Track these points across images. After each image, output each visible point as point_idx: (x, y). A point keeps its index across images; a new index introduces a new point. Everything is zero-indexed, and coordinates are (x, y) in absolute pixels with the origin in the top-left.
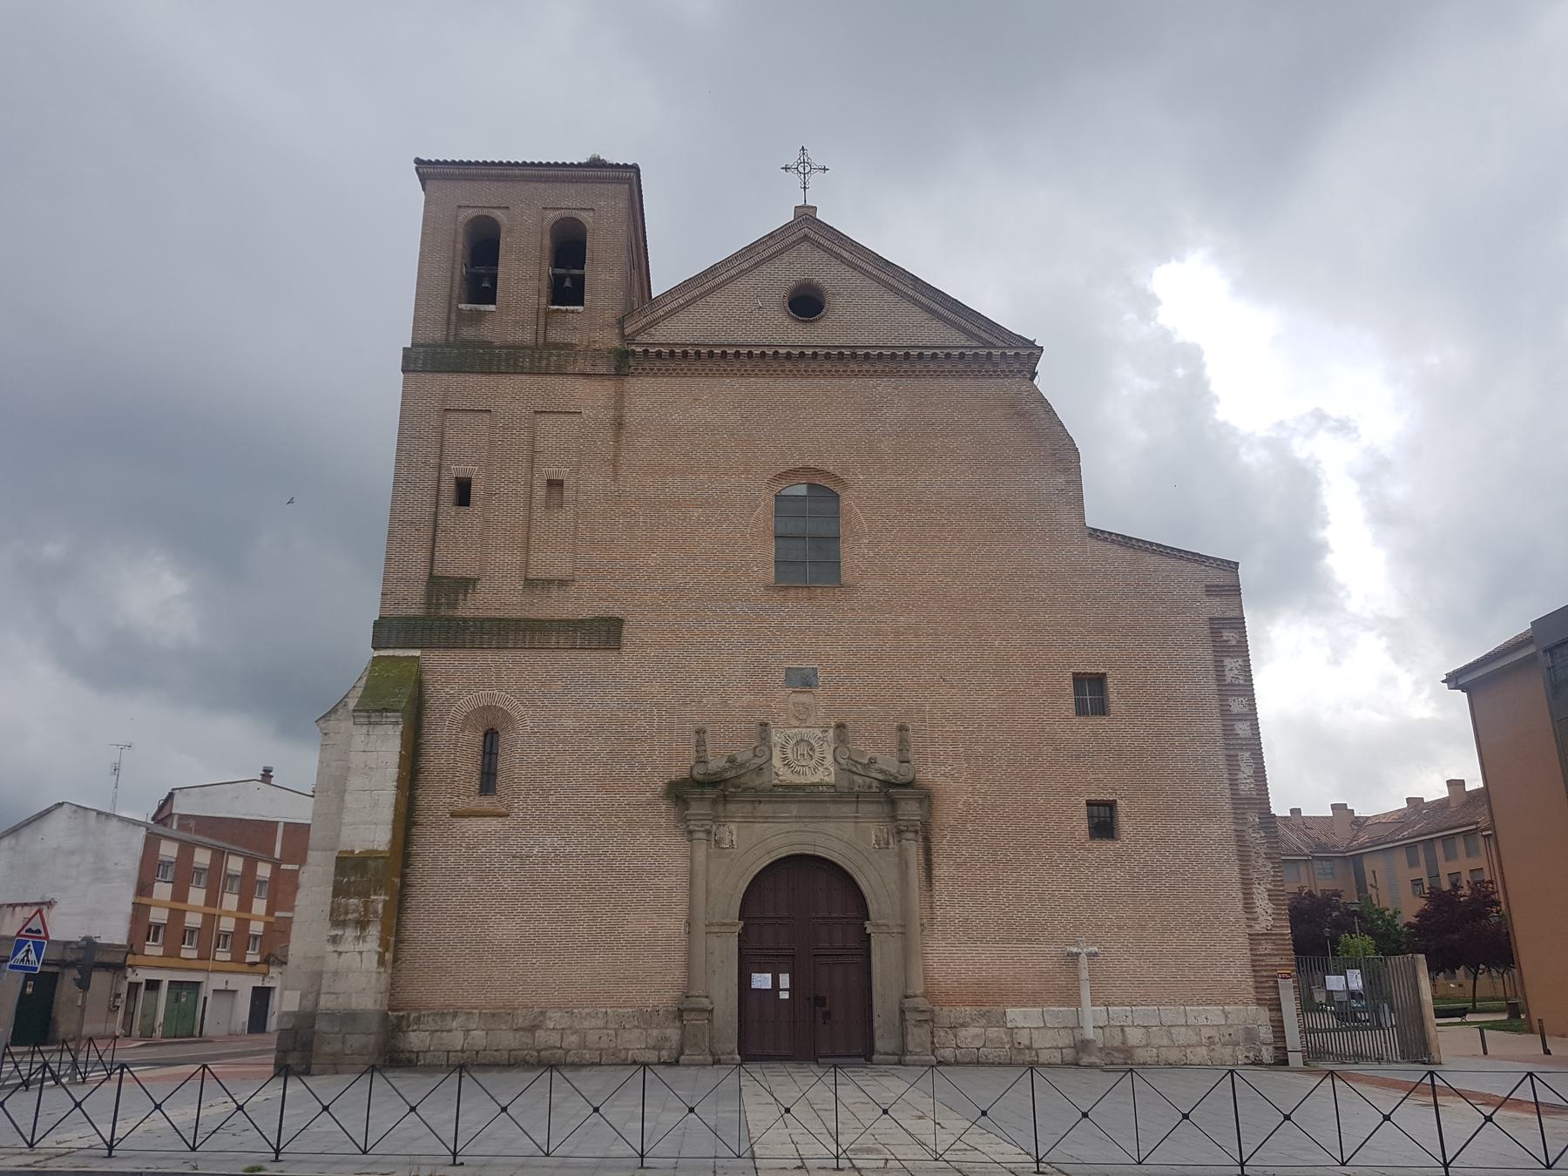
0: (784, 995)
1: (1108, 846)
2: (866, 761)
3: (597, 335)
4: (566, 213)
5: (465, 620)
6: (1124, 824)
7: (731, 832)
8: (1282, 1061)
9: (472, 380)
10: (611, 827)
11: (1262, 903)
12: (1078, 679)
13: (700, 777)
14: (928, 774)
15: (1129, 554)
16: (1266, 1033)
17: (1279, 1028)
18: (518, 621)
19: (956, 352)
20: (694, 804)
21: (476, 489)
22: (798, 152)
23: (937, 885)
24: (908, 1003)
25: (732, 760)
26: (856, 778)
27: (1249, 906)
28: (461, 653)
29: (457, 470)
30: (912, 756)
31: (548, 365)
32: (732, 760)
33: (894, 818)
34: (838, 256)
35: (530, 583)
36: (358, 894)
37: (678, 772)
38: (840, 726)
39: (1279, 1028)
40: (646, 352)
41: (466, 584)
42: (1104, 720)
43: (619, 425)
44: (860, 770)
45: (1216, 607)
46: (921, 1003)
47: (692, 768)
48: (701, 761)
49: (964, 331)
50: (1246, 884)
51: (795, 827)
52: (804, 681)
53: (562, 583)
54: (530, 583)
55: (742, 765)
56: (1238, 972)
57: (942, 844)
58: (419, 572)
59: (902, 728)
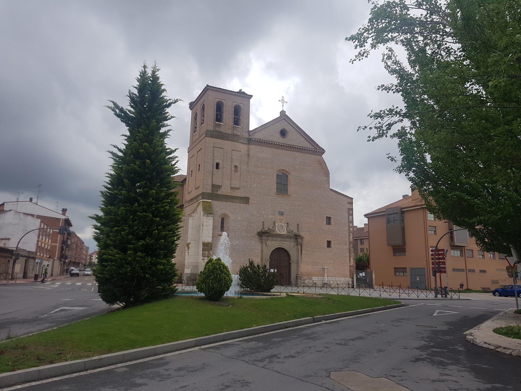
1: (330, 249)
2: (292, 230)
3: (244, 134)
4: (237, 104)
5: (220, 195)
6: (332, 245)
7: (269, 242)
8: (353, 287)
9: (220, 141)
10: (247, 240)
11: (352, 260)
12: (327, 217)
13: (264, 232)
14: (302, 234)
15: (336, 194)
16: (351, 283)
17: (353, 282)
18: (230, 196)
19: (311, 149)
20: (263, 237)
21: (220, 166)
22: (282, 98)
23: (303, 255)
24: (298, 276)
25: (269, 228)
26: (290, 234)
27: (350, 261)
28: (219, 202)
29: (217, 161)
30: (299, 230)
31: (235, 140)
32: (269, 228)
33: (297, 242)
34: (290, 124)
35: (232, 188)
37: (259, 230)
38: (288, 223)
39: (353, 282)
40: (255, 140)
41: (219, 187)
42: (330, 226)
43: (249, 155)
44: (290, 232)
45: (349, 206)
46: (300, 275)
48: (263, 228)
49: (311, 144)
50: (350, 257)
51: (280, 242)
52: (281, 214)
53: (238, 189)
54: (232, 188)
55: (271, 230)
56: (348, 273)
57: (304, 247)
58: (210, 183)
59: (298, 225)
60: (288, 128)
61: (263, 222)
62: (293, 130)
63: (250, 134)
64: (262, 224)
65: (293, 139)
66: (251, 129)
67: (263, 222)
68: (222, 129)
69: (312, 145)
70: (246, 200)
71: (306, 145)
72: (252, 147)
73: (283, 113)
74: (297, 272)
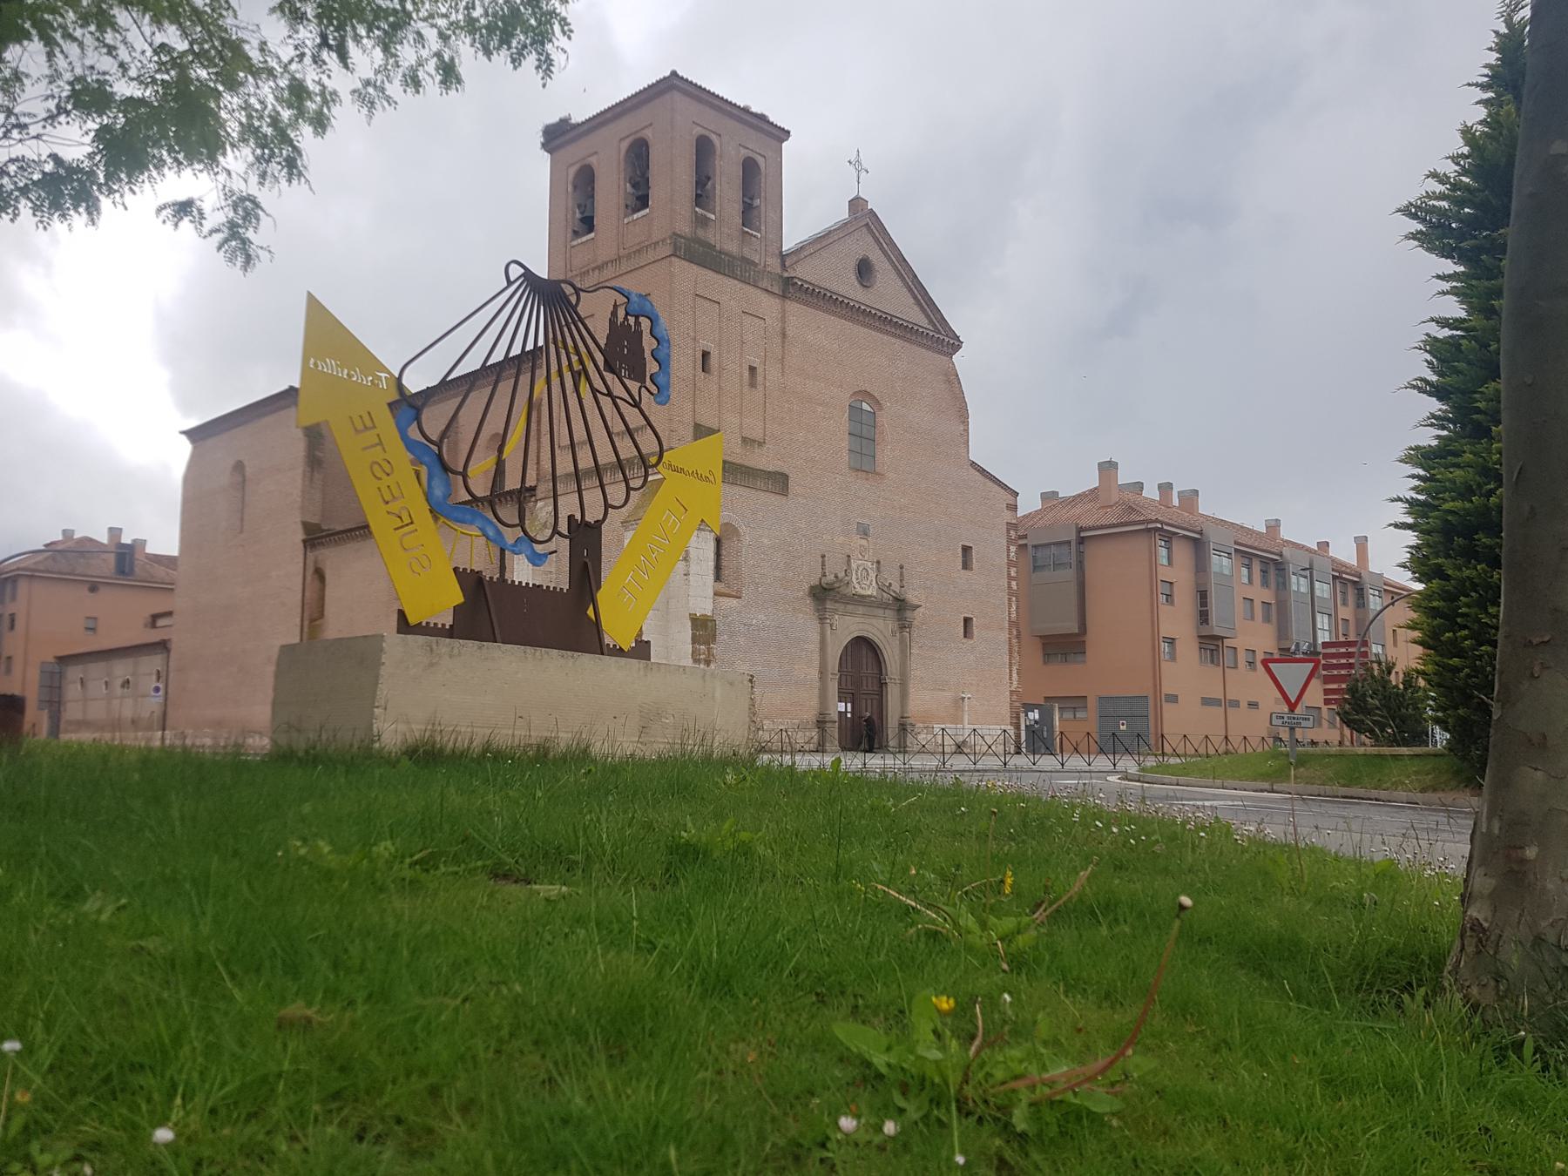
0: (849, 715)
14: (911, 597)
20: (828, 602)
25: (836, 577)
29: (705, 344)
32: (836, 577)
35: (744, 440)
36: (704, 643)
37: (814, 581)
43: (784, 335)
44: (885, 589)
47: (820, 579)
49: (928, 316)
50: (1011, 665)
51: (862, 620)
52: (864, 532)
54: (744, 440)
55: (841, 581)
56: (1005, 711)
58: (688, 419)
60: (876, 257)
61: (823, 557)
62: (887, 265)
63: (787, 264)
64: (820, 560)
65: (887, 295)
66: (788, 244)
67: (823, 557)
68: (711, 236)
69: (931, 322)
70: (779, 482)
71: (915, 316)
72: (793, 307)
73: (856, 204)
74: (903, 712)
